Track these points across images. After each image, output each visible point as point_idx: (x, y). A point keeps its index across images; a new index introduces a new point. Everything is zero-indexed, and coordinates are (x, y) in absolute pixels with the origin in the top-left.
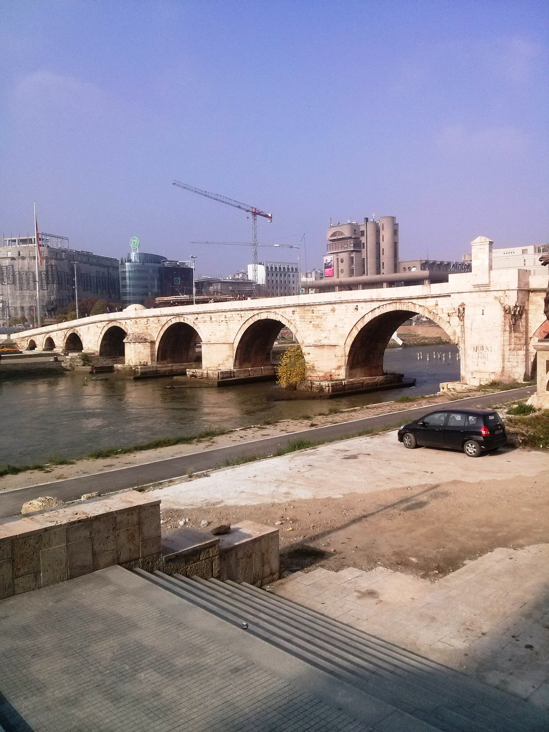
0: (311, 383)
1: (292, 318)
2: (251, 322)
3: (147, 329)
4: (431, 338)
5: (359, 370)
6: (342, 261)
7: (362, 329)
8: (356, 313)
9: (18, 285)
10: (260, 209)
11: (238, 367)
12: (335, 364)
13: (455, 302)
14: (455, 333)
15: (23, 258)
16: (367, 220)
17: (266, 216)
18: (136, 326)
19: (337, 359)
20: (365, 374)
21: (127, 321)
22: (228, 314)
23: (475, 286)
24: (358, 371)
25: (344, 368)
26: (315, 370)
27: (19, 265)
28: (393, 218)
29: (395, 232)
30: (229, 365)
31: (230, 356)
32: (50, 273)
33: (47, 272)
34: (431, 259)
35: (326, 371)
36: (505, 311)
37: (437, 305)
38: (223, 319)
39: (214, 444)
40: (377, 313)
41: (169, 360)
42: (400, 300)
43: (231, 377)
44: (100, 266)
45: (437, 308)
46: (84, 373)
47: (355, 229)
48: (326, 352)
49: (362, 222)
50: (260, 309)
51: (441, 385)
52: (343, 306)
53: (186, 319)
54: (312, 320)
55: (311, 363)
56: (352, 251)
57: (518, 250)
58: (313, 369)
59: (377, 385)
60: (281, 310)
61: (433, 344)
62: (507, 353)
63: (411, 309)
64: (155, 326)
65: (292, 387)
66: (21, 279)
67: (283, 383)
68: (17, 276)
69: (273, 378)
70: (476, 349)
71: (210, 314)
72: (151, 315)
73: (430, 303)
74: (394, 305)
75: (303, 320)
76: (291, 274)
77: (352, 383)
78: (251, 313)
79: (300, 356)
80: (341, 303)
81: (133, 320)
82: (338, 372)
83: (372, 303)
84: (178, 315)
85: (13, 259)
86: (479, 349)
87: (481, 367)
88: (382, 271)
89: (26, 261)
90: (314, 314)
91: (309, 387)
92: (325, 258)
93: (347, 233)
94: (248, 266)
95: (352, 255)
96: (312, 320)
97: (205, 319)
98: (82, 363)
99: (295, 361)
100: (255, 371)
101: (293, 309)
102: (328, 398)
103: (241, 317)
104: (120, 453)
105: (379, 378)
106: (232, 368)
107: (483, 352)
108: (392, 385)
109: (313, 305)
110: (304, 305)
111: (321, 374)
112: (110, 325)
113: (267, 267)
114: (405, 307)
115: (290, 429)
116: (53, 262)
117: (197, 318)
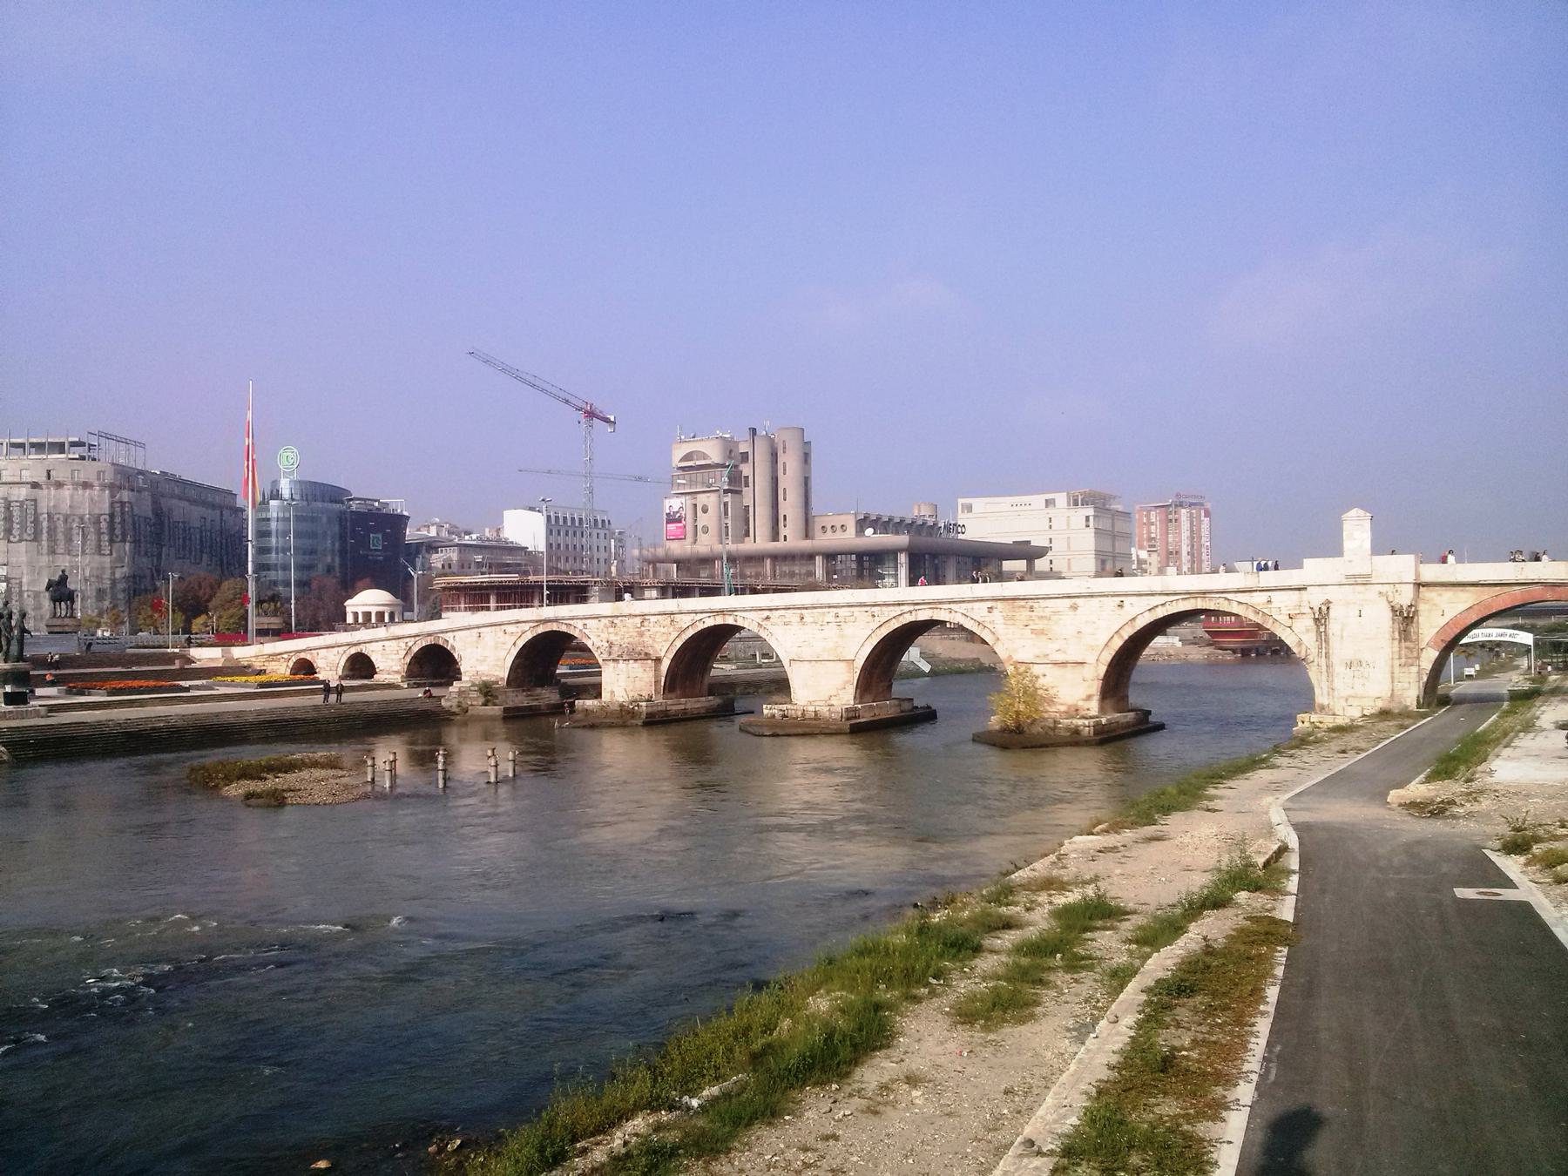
3: (641, 635)
6: (705, 510)
8: (1120, 611)
9: (45, 543)
10: (599, 407)
13: (1315, 598)
14: (1300, 643)
15: (59, 485)
16: (754, 431)
17: (607, 420)
22: (843, 612)
23: (1348, 577)
27: (47, 499)
29: (806, 458)
32: (118, 520)
33: (112, 516)
36: (1393, 609)
44: (205, 504)
46: (480, 719)
48: (1069, 672)
51: (1300, 717)
56: (726, 491)
57: (1038, 500)
58: (1051, 701)
62: (1397, 670)
63: (1224, 607)
66: (52, 531)
68: (45, 524)
72: (653, 611)
73: (1258, 599)
78: (898, 610)
82: (1086, 705)
84: (722, 612)
85: (35, 485)
88: (783, 532)
89: (66, 492)
92: (667, 503)
93: (715, 456)
94: (506, 513)
98: (482, 700)
101: (990, 604)
111: (1063, 708)
113: (549, 517)
116: (125, 495)
117: (768, 618)
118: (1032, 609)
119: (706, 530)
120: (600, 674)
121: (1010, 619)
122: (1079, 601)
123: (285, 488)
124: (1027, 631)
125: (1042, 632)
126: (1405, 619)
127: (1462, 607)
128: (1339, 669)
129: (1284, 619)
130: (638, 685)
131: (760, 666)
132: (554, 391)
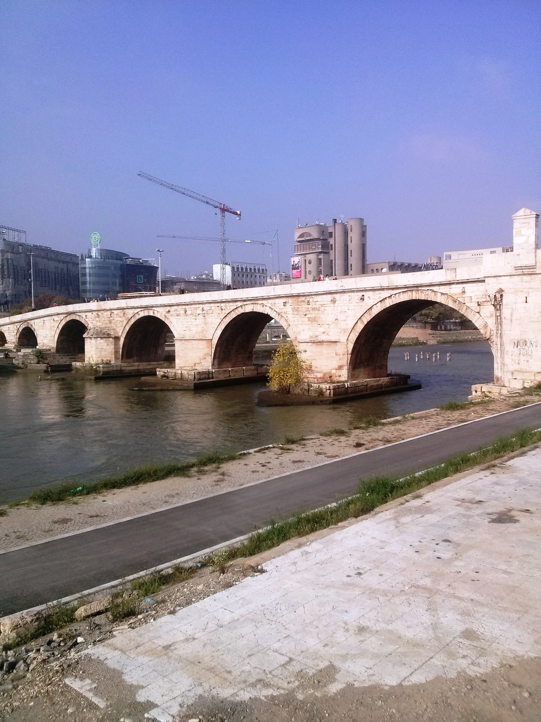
0: (309, 385)
1: (283, 311)
2: (233, 315)
3: (110, 322)
4: (408, 338)
5: (362, 370)
6: (310, 262)
7: (368, 323)
8: (363, 303)
10: (229, 205)
11: (217, 367)
12: (335, 363)
13: (492, 287)
14: (486, 326)
16: (335, 221)
17: (236, 213)
18: (97, 319)
19: (338, 357)
20: (368, 375)
21: (87, 314)
22: (206, 307)
23: (516, 268)
24: (361, 371)
25: (346, 368)
26: (312, 370)
28: (362, 220)
29: (363, 234)
30: (206, 364)
31: (207, 354)
32: (5, 267)
34: (399, 261)
35: (324, 372)
37: (464, 292)
38: (200, 312)
39: (226, 477)
40: (388, 303)
41: (136, 358)
42: (417, 287)
43: (209, 378)
44: (59, 261)
45: (464, 296)
47: (322, 230)
48: (325, 349)
49: (330, 223)
50: (244, 301)
51: (473, 387)
52: (346, 296)
53: (156, 312)
54: (308, 312)
55: (308, 363)
56: (320, 253)
58: (310, 369)
59: (382, 388)
61: (410, 345)
63: (431, 297)
64: (120, 319)
65: (285, 390)
67: (274, 386)
69: (262, 379)
70: (517, 344)
71: (184, 307)
72: (115, 307)
73: (456, 290)
74: (409, 293)
75: (296, 313)
76: (258, 275)
77: (356, 386)
78: (233, 306)
79: (293, 353)
80: (344, 292)
81: (95, 313)
82: (338, 373)
83: (382, 292)
84: (146, 308)
86: (522, 344)
87: (524, 366)
90: (310, 306)
91: (305, 390)
92: (292, 259)
93: (315, 234)
95: (320, 257)
96: (308, 312)
97: (178, 313)
98: (36, 360)
99: (289, 360)
100: (236, 372)
101: (284, 300)
102: (330, 404)
103: (222, 309)
104: (81, 493)
105: (384, 380)
106: (210, 368)
107: (526, 348)
108: (398, 387)
109: (308, 295)
110: (298, 296)
111: (319, 375)
112: (68, 319)
113: (233, 268)
114: (423, 295)
115: (330, 450)
116: (9, 256)
117: (169, 311)
120: (174, 345)
121: (296, 310)
122: (337, 296)
123: (94, 253)
129: (473, 305)
130: (103, 353)
131: (268, 342)
132: (201, 197)
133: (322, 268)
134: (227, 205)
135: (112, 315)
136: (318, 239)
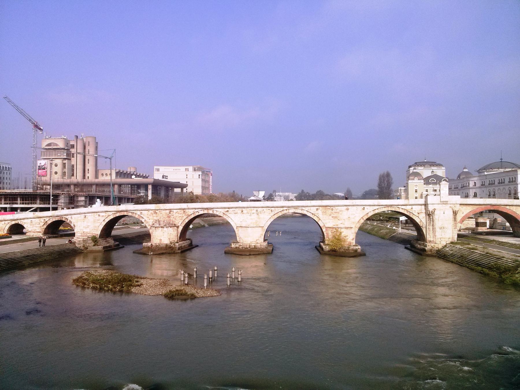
3: (169, 217)
6: (56, 165)
8: (363, 211)
18: (155, 215)
36: (453, 212)
38: (255, 212)
40: (377, 211)
46: (92, 252)
57: (183, 168)
58: (345, 241)
60: (307, 208)
64: (179, 215)
70: (441, 228)
73: (408, 208)
76: (5, 172)
78: (282, 209)
87: (443, 236)
88: (87, 175)
93: (61, 145)
95: (64, 162)
98: (93, 244)
101: (317, 208)
117: (228, 211)
118: (332, 210)
119: (56, 173)
121: (324, 213)
124: (331, 217)
125: (336, 217)
126: (455, 213)
127: (468, 211)
128: (438, 230)
129: (416, 214)
130: (172, 237)
133: (66, 170)
134: (38, 123)
135: (171, 213)
136: (64, 149)
